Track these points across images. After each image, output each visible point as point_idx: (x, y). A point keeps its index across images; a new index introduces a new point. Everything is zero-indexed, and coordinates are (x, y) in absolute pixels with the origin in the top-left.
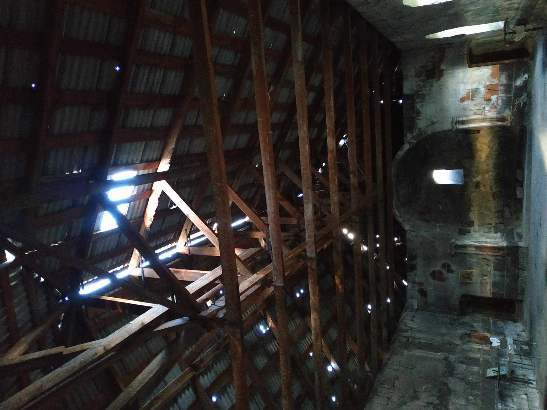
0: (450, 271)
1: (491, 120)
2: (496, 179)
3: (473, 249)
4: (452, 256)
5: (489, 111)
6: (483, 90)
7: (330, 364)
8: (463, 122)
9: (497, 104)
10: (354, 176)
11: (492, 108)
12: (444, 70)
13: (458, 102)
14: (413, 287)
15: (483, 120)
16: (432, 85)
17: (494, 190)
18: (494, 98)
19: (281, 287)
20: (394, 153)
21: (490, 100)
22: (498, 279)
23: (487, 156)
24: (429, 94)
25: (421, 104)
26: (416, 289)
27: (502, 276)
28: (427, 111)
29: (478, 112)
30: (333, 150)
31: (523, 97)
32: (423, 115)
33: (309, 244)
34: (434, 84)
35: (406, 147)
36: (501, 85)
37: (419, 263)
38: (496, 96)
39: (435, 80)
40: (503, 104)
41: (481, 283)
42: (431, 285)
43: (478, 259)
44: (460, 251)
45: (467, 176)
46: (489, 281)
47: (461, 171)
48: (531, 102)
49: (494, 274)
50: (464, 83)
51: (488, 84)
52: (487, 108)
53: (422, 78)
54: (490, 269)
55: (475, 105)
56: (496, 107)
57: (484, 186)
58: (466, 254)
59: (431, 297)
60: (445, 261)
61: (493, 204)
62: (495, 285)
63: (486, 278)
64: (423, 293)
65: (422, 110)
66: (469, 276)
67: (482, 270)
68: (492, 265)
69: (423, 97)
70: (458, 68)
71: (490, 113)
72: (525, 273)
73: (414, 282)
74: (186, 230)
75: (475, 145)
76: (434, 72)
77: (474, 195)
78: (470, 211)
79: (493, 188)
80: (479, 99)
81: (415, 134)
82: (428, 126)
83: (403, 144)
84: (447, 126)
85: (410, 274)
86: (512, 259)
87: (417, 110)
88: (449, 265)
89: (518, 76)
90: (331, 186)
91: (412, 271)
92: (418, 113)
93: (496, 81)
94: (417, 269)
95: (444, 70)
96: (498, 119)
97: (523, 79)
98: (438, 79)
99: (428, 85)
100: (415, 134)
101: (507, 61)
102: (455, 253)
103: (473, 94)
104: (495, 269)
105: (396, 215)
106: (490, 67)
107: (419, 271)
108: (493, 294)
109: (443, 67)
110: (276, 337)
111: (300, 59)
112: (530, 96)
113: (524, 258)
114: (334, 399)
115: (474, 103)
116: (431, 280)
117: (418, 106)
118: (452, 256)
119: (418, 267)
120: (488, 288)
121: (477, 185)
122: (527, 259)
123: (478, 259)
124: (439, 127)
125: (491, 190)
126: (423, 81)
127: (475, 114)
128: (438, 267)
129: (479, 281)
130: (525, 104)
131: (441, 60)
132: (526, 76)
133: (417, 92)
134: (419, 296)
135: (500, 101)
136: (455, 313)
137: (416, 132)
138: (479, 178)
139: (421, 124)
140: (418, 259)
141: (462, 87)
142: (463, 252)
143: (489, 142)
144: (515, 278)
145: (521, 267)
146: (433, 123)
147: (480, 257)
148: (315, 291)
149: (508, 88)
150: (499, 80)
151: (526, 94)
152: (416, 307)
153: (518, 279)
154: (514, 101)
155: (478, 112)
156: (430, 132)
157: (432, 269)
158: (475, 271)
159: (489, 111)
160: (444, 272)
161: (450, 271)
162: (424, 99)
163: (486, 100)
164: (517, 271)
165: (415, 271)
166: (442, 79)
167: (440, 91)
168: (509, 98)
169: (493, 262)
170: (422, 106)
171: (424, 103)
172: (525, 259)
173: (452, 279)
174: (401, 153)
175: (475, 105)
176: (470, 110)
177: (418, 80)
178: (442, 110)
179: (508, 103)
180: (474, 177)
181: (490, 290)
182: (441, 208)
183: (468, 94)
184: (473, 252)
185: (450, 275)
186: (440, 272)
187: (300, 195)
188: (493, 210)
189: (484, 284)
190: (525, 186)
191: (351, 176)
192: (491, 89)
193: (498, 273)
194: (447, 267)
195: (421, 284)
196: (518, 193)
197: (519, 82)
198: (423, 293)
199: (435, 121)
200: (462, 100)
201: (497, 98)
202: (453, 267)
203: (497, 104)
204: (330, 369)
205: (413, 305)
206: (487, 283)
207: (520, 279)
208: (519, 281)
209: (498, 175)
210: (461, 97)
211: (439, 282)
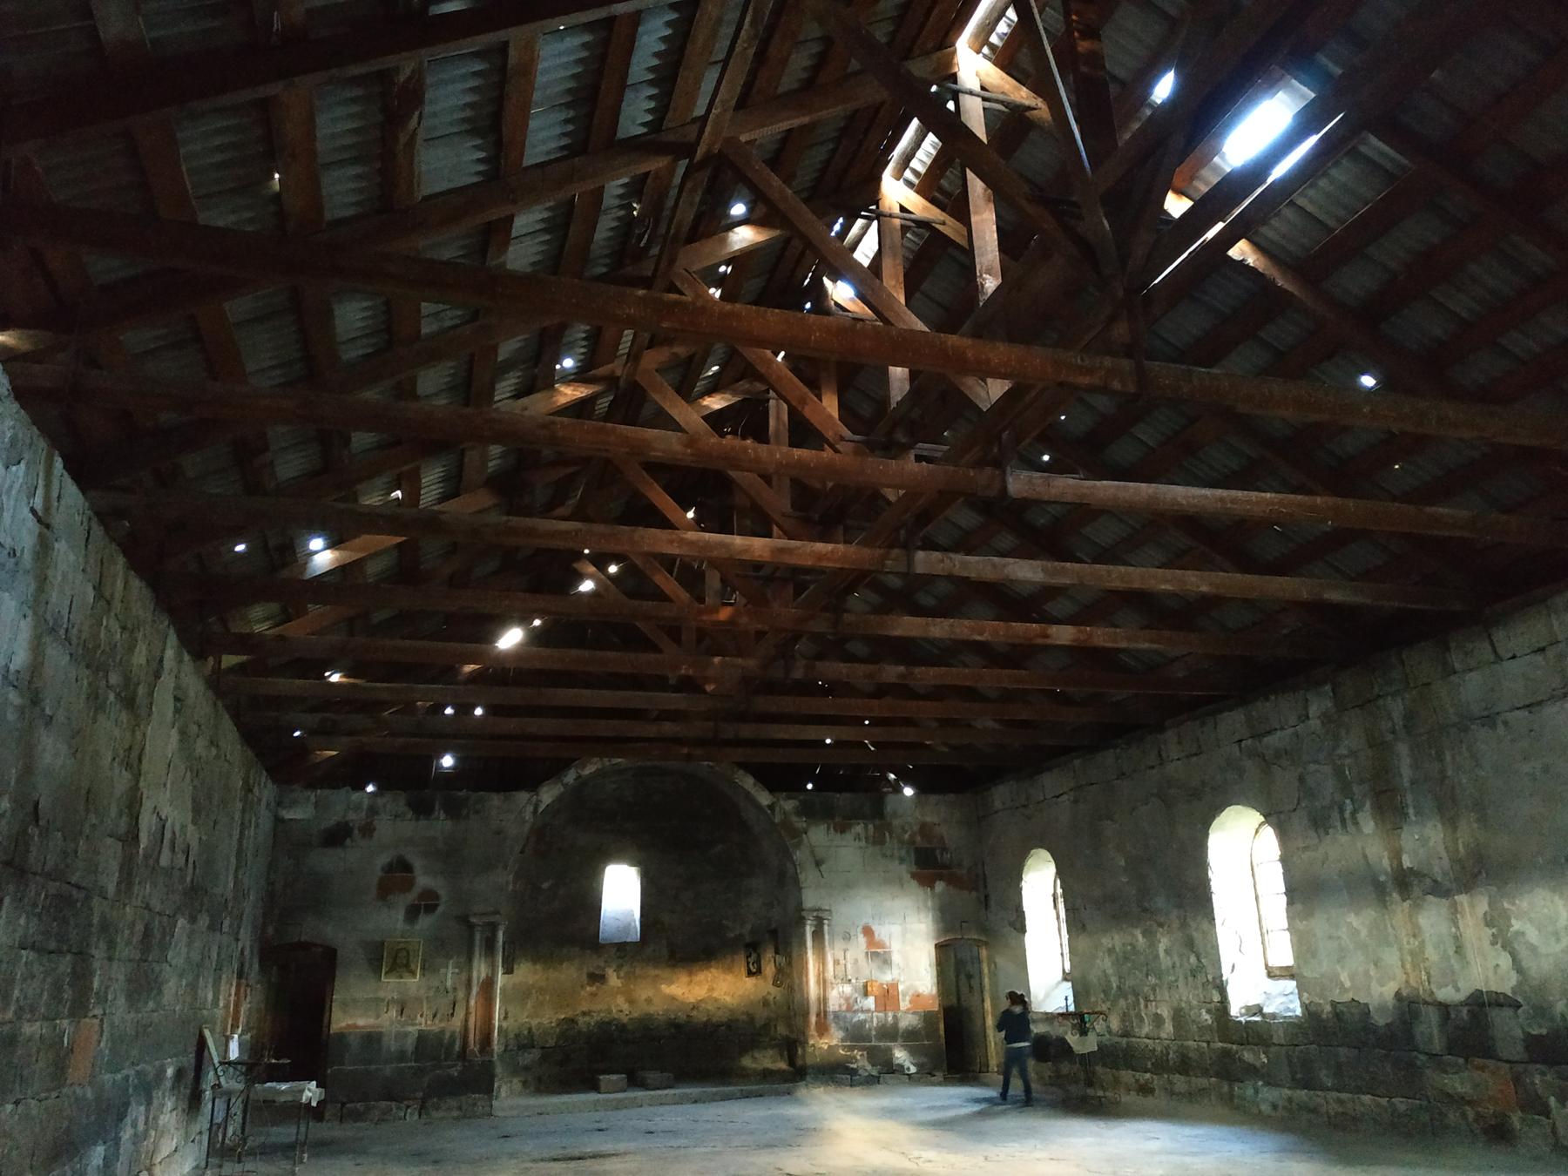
0: (413, 913)
1: (823, 1000)
2: (609, 1023)
3: (483, 975)
4: (464, 920)
5: (841, 995)
6: (887, 978)
7: (331, 545)
8: (818, 935)
9: (856, 1012)
10: (902, 676)
11: (847, 999)
12: (932, 888)
13: (861, 924)
14: (358, 807)
15: (823, 982)
16: (902, 860)
17: (581, 1020)
18: (870, 1002)
19: (1004, 489)
20: (748, 767)
21: (866, 994)
22: (391, 1045)
23: (673, 998)
24: (884, 856)
25: (863, 835)
26: (352, 816)
27: (401, 1056)
28: (846, 849)
29: (840, 968)
30: (1047, 636)
31: (869, 1067)
32: (838, 839)
33: (947, 561)
34: (904, 867)
35: (764, 798)
36: (895, 1017)
37: (440, 826)
38: (873, 1007)
39: (914, 869)
40: (854, 1026)
41: (378, 1000)
42: (363, 862)
43: (455, 989)
44: (478, 936)
45: (624, 952)
46: (386, 1021)
47: (636, 935)
48: (860, 1084)
49: (406, 1035)
50: (904, 933)
51: (901, 988)
52: (847, 989)
53: (918, 839)
54: (423, 1023)
55: (856, 961)
56: (849, 1009)
57: (594, 995)
58: (470, 960)
59: (328, 861)
60: (444, 898)
61: (547, 1019)
62: (372, 1039)
63: (393, 1013)
64: (337, 836)
65: (849, 836)
66: (400, 963)
67: (418, 1000)
68: (434, 1026)
69: (878, 841)
70: (935, 921)
71: (837, 996)
72: (412, 1117)
73: (373, 811)
74: (944, 223)
75: (708, 968)
76: (929, 865)
77: (569, 973)
78: (535, 962)
79: (587, 1019)
80: (869, 970)
81: (794, 819)
82: (812, 852)
83: (772, 790)
84: (810, 899)
85: (402, 802)
86: (451, 1077)
87: (849, 827)
88: (431, 909)
89: (912, 1051)
90: (966, 622)
91: (409, 804)
92: (842, 829)
93: (904, 1004)
94: (417, 820)
95: (932, 888)
96: (823, 1014)
97: (907, 1064)
98: (914, 876)
99: (903, 853)
100: (794, 819)
101: (942, 1026)
102: (471, 927)
103: (879, 954)
104: (422, 1037)
105: (584, 767)
106: (934, 991)
107: (409, 827)
108: (341, 1036)
109: (940, 886)
110: (525, 401)
111: (1326, 596)
112: (871, 1081)
113: (460, 1108)
114: (240, 548)
115: (861, 957)
116: (383, 860)
117: (859, 828)
118: (464, 920)
119: (423, 823)
120: (361, 1022)
121: (597, 978)
122: (457, 1119)
123: (455, 989)
124: (808, 877)
125: (584, 1014)
126: (912, 842)
127: (836, 962)
128: (423, 881)
129: (381, 994)
130: (854, 1072)
131: (953, 881)
132: (913, 1070)
133: (889, 827)
134: (325, 825)
135: (862, 1016)
136: (270, 930)
137: (800, 823)
138: (614, 980)
139: (818, 835)
140: (449, 823)
141: (896, 929)
142: (477, 949)
143: (716, 1000)
144: (393, 1092)
145: (429, 1104)
146: (818, 864)
147: (461, 994)
148: (829, 560)
149: (889, 1033)
150: (907, 1012)
151: (875, 1073)
152: (288, 814)
153: (391, 1099)
154: (862, 1049)
155: (840, 968)
156: (798, 855)
157: (418, 864)
158: (414, 983)
159: (841, 995)
160: (411, 897)
161: (413, 913)
162: (874, 843)
163: (865, 986)
164: (420, 1095)
165: (410, 815)
166: (914, 883)
167: (890, 881)
168: (867, 1038)
169: (442, 1032)
170: (857, 837)
171: (863, 843)
172: (455, 1113)
173: (390, 921)
174: (748, 782)
175: (856, 961)
176: (845, 951)
177: (916, 828)
178: (849, 885)
179: (856, 1035)
180: (619, 968)
181: (355, 1026)
182: (545, 885)
183: (881, 945)
184: (475, 975)
185: (401, 916)
186: (408, 885)
187: (690, 515)
188: (534, 1022)
189: (366, 1009)
190: (631, 1094)
191: (902, 669)
192: (888, 996)
193: (410, 1044)
194: (428, 902)
195: (368, 830)
196: (614, 1077)
197: (900, 1055)
198: (337, 836)
199: (823, 868)
200: (868, 932)
201: (868, 1011)
202: (425, 922)
203: (856, 1012)
204: (316, 543)
205: (294, 804)
206: (378, 1017)
207: (393, 1104)
208: (383, 1104)
209: (622, 1028)
210: (874, 928)
211: (375, 881)
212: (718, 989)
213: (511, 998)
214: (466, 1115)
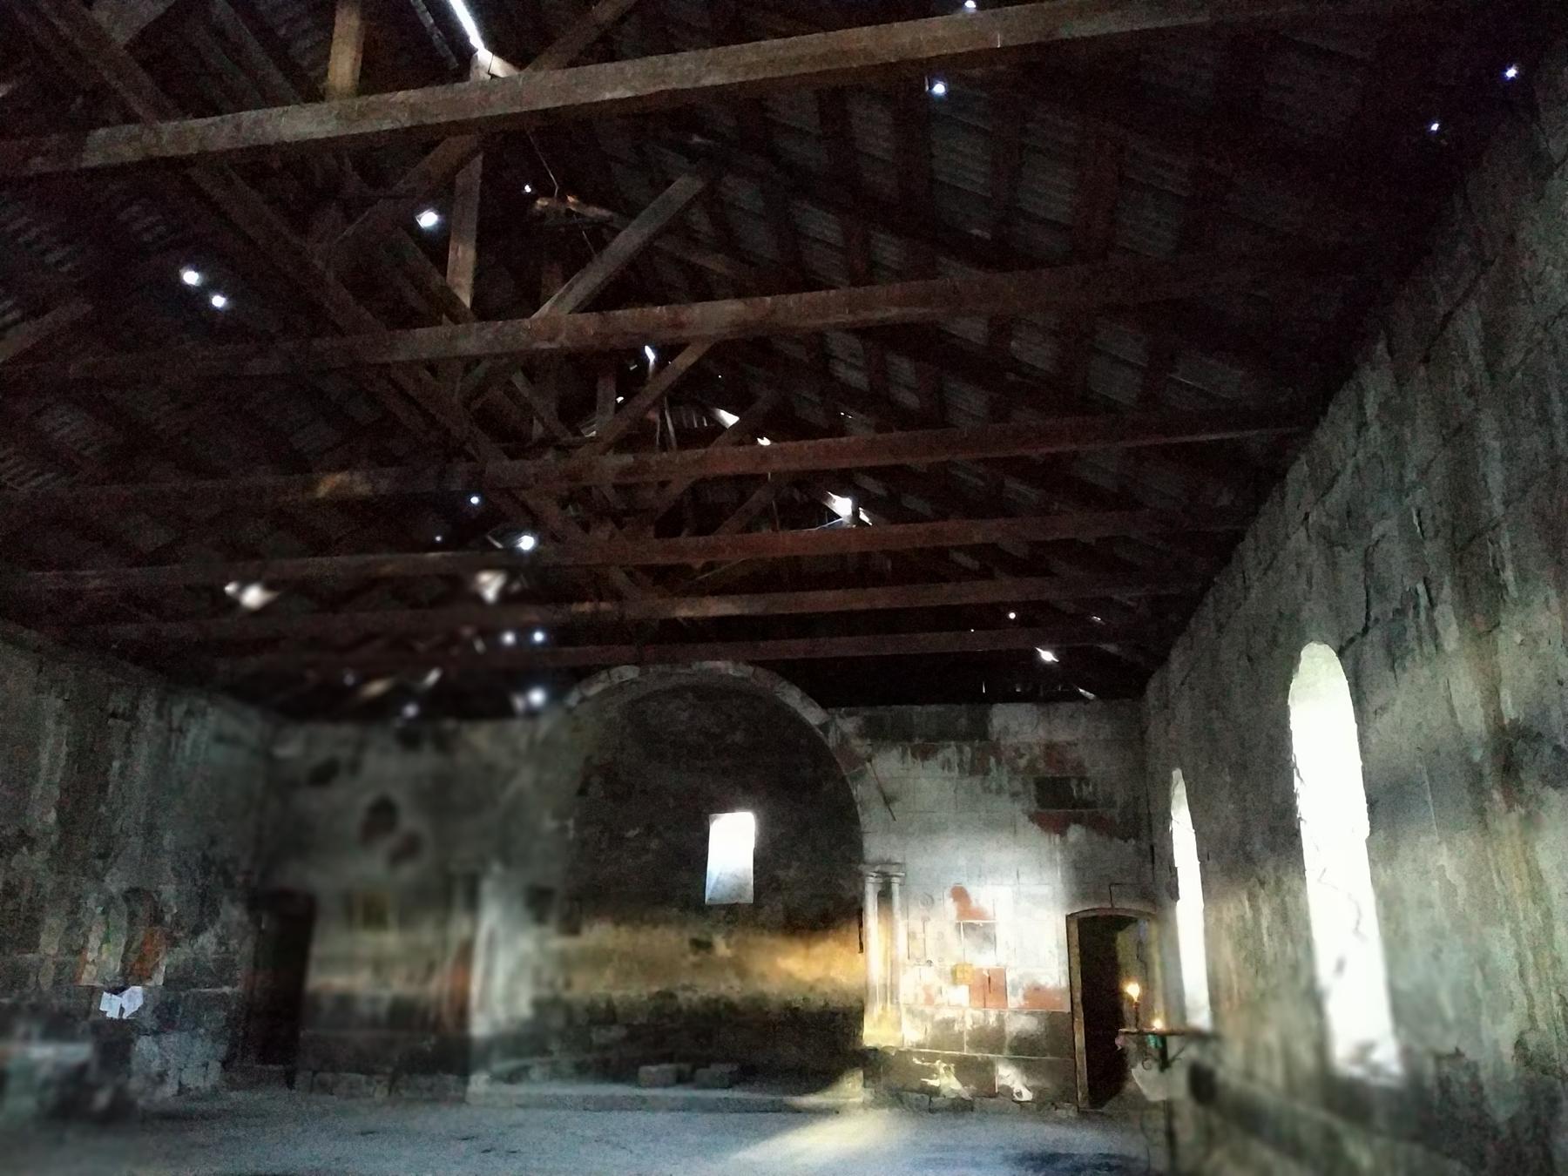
2: (717, 1001)
6: (985, 961)
8: (885, 896)
10: (626, 471)
12: (1063, 834)
13: (953, 880)
15: (893, 965)
17: (682, 996)
22: (364, 1009)
23: (790, 975)
24: (987, 790)
25: (955, 759)
27: (374, 1022)
28: (927, 781)
30: (680, 326)
34: (1018, 806)
35: (813, 715)
36: (1000, 1018)
39: (1034, 807)
42: (348, 801)
45: (732, 914)
46: (359, 982)
47: (749, 897)
52: (930, 976)
53: (1041, 765)
54: (398, 986)
55: (941, 935)
56: (929, 1000)
57: (697, 966)
59: (313, 802)
61: (636, 991)
62: (345, 1001)
65: (933, 764)
69: (977, 768)
72: (380, 1094)
75: (824, 938)
76: (1056, 802)
77: (665, 940)
78: (617, 924)
79: (689, 994)
84: (875, 847)
86: (428, 1051)
87: (935, 751)
89: (1028, 1068)
92: (925, 754)
95: (1063, 834)
98: (1035, 818)
99: (1018, 786)
101: (1080, 1039)
103: (974, 924)
105: (590, 685)
106: (1064, 983)
109: (1075, 833)
115: (949, 930)
116: (367, 799)
117: (949, 752)
121: (702, 945)
124: (871, 818)
125: (685, 988)
126: (1031, 767)
127: (911, 936)
128: (410, 821)
131: (1096, 824)
133: (995, 749)
137: (860, 746)
138: (722, 948)
139: (889, 765)
143: (833, 980)
144: (365, 1064)
146: (888, 801)
149: (991, 1040)
153: (358, 1071)
156: (859, 791)
158: (390, 940)
162: (973, 772)
164: (389, 1070)
167: (992, 825)
170: (946, 765)
171: (956, 773)
173: (370, 868)
174: (793, 697)
175: (941, 935)
177: (1037, 751)
178: (931, 829)
180: (728, 935)
182: (631, 833)
183: (979, 914)
188: (617, 994)
189: (355, 970)
191: (628, 459)
192: (991, 987)
193: (383, 1009)
194: (409, 849)
196: (653, 1069)
198: (324, 775)
199: (896, 806)
200: (960, 895)
201: (959, 1006)
203: (938, 1007)
207: (363, 1078)
208: (354, 1076)
209: (731, 1007)
212: (800, 969)
213: (618, 963)
214: (437, 1098)
